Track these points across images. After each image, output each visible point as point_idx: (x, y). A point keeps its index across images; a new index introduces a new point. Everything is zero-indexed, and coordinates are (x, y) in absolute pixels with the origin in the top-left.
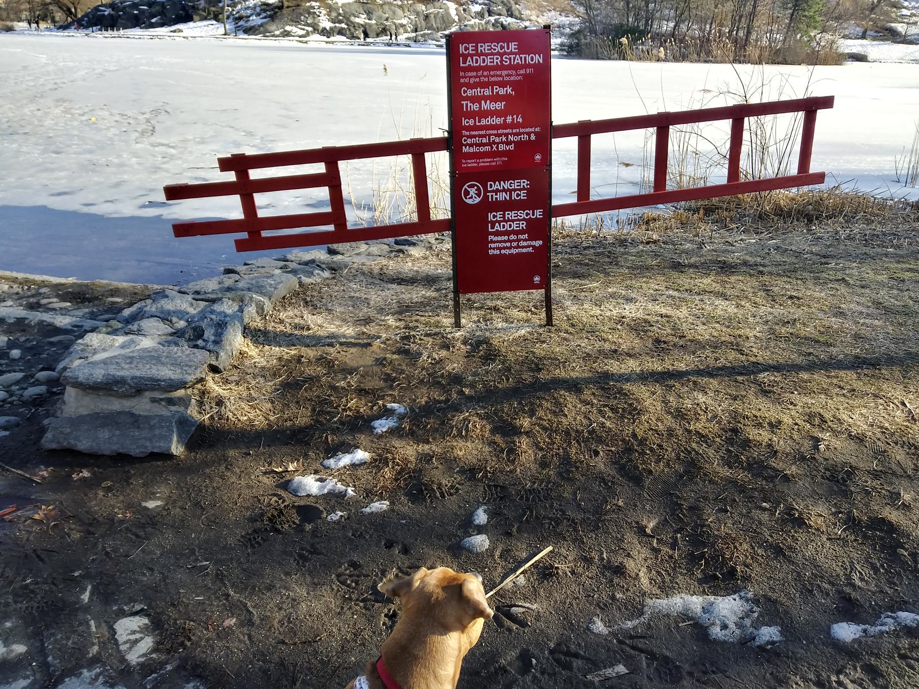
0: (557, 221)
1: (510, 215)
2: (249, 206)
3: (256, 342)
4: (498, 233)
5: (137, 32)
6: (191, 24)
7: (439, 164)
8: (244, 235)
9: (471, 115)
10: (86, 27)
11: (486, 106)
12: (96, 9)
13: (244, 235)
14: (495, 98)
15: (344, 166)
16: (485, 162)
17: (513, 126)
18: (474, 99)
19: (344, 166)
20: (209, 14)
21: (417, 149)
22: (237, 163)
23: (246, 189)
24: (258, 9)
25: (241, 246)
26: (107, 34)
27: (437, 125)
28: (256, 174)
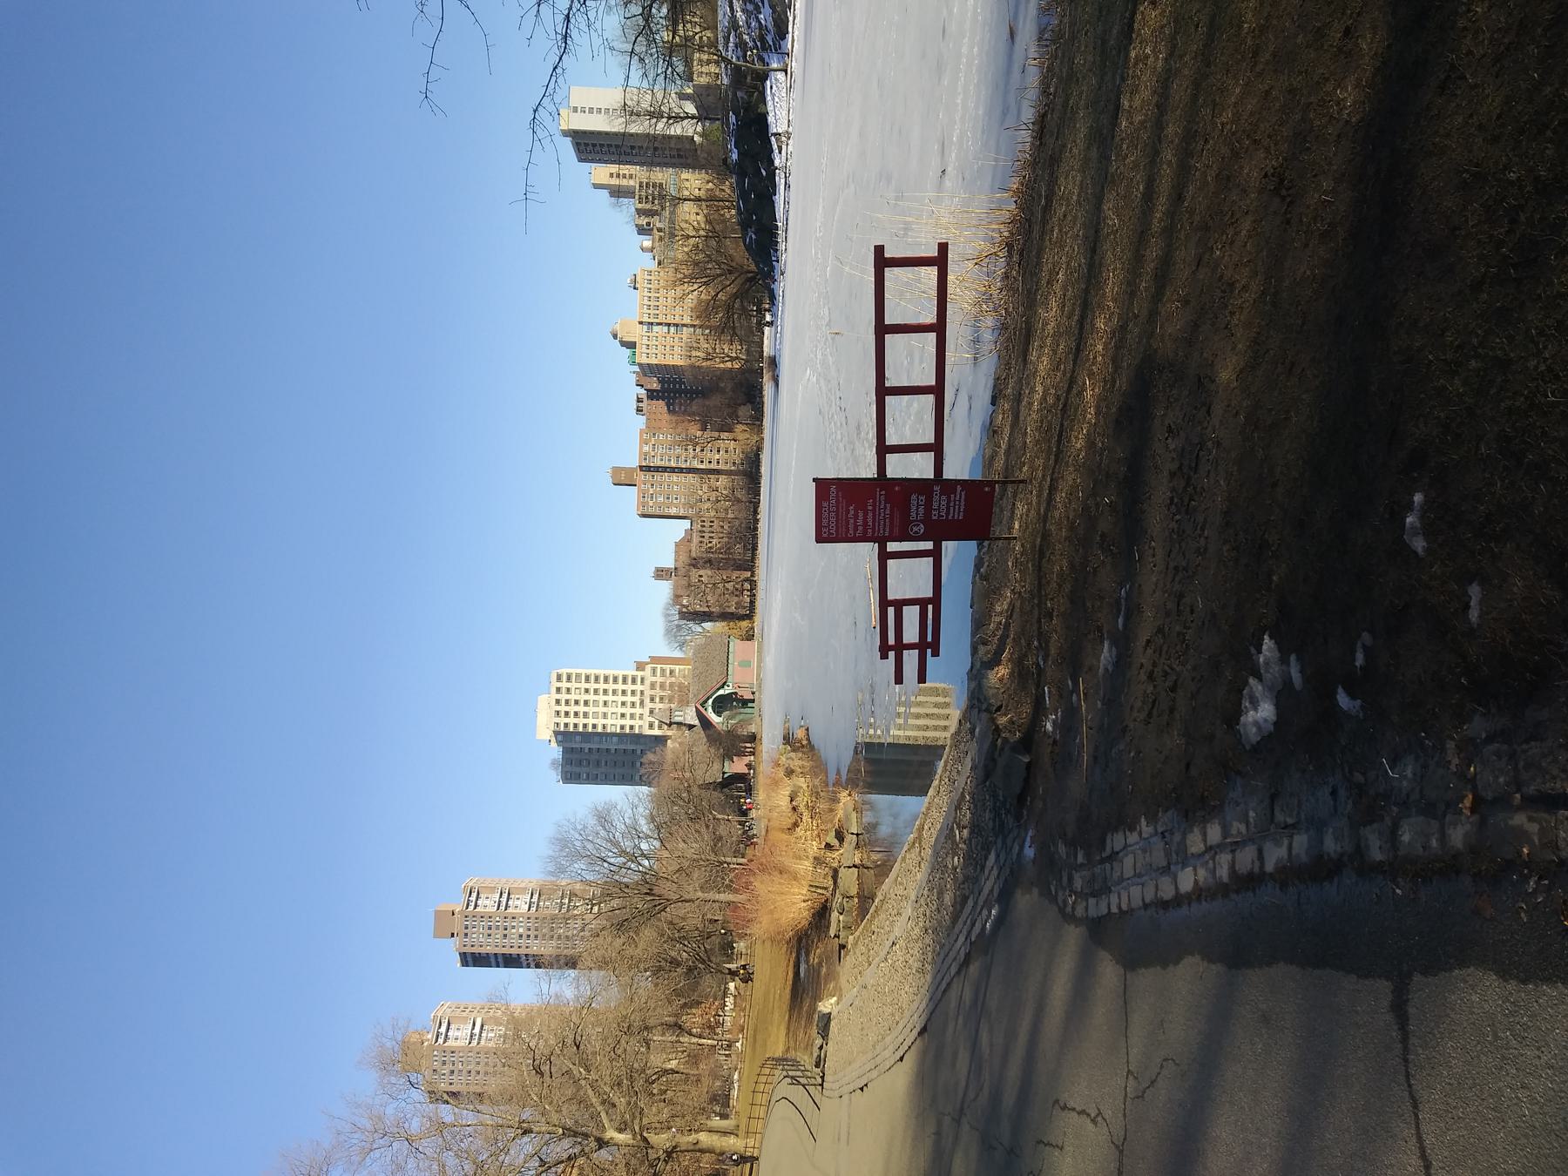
0: (949, 474)
1: (935, 505)
2: (911, 646)
3: (998, 664)
4: (948, 514)
5: (779, 199)
6: (771, 119)
7: (892, 547)
8: (929, 651)
9: (865, 531)
10: (772, 268)
11: (860, 522)
12: (748, 248)
13: (929, 651)
14: (856, 517)
15: (890, 597)
16: (897, 521)
17: (874, 506)
18: (856, 529)
19: (890, 597)
20: (756, 88)
21: (884, 557)
22: (884, 651)
23: (900, 647)
24: (750, 7)
25: (936, 654)
26: (782, 247)
27: (868, 550)
28: (891, 641)
